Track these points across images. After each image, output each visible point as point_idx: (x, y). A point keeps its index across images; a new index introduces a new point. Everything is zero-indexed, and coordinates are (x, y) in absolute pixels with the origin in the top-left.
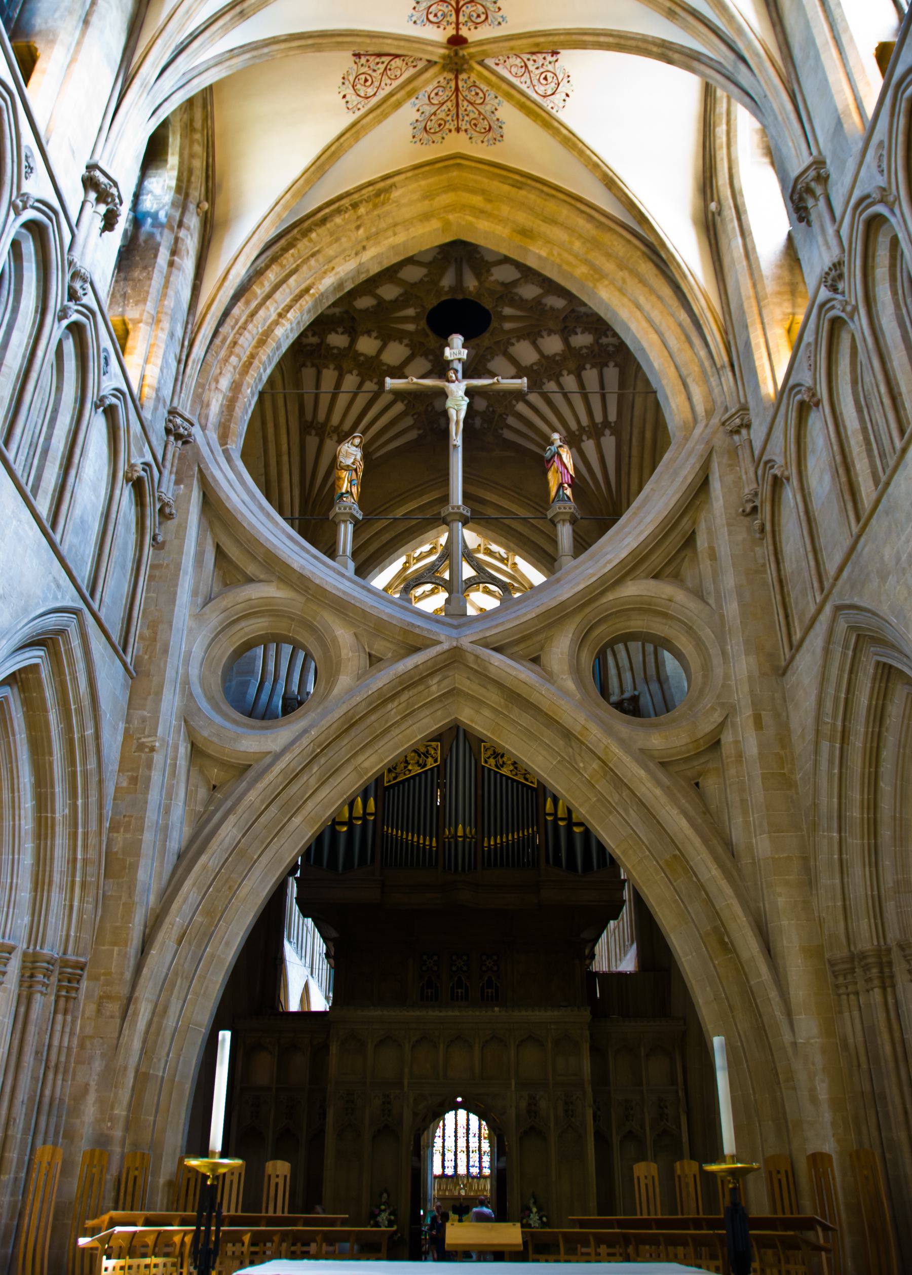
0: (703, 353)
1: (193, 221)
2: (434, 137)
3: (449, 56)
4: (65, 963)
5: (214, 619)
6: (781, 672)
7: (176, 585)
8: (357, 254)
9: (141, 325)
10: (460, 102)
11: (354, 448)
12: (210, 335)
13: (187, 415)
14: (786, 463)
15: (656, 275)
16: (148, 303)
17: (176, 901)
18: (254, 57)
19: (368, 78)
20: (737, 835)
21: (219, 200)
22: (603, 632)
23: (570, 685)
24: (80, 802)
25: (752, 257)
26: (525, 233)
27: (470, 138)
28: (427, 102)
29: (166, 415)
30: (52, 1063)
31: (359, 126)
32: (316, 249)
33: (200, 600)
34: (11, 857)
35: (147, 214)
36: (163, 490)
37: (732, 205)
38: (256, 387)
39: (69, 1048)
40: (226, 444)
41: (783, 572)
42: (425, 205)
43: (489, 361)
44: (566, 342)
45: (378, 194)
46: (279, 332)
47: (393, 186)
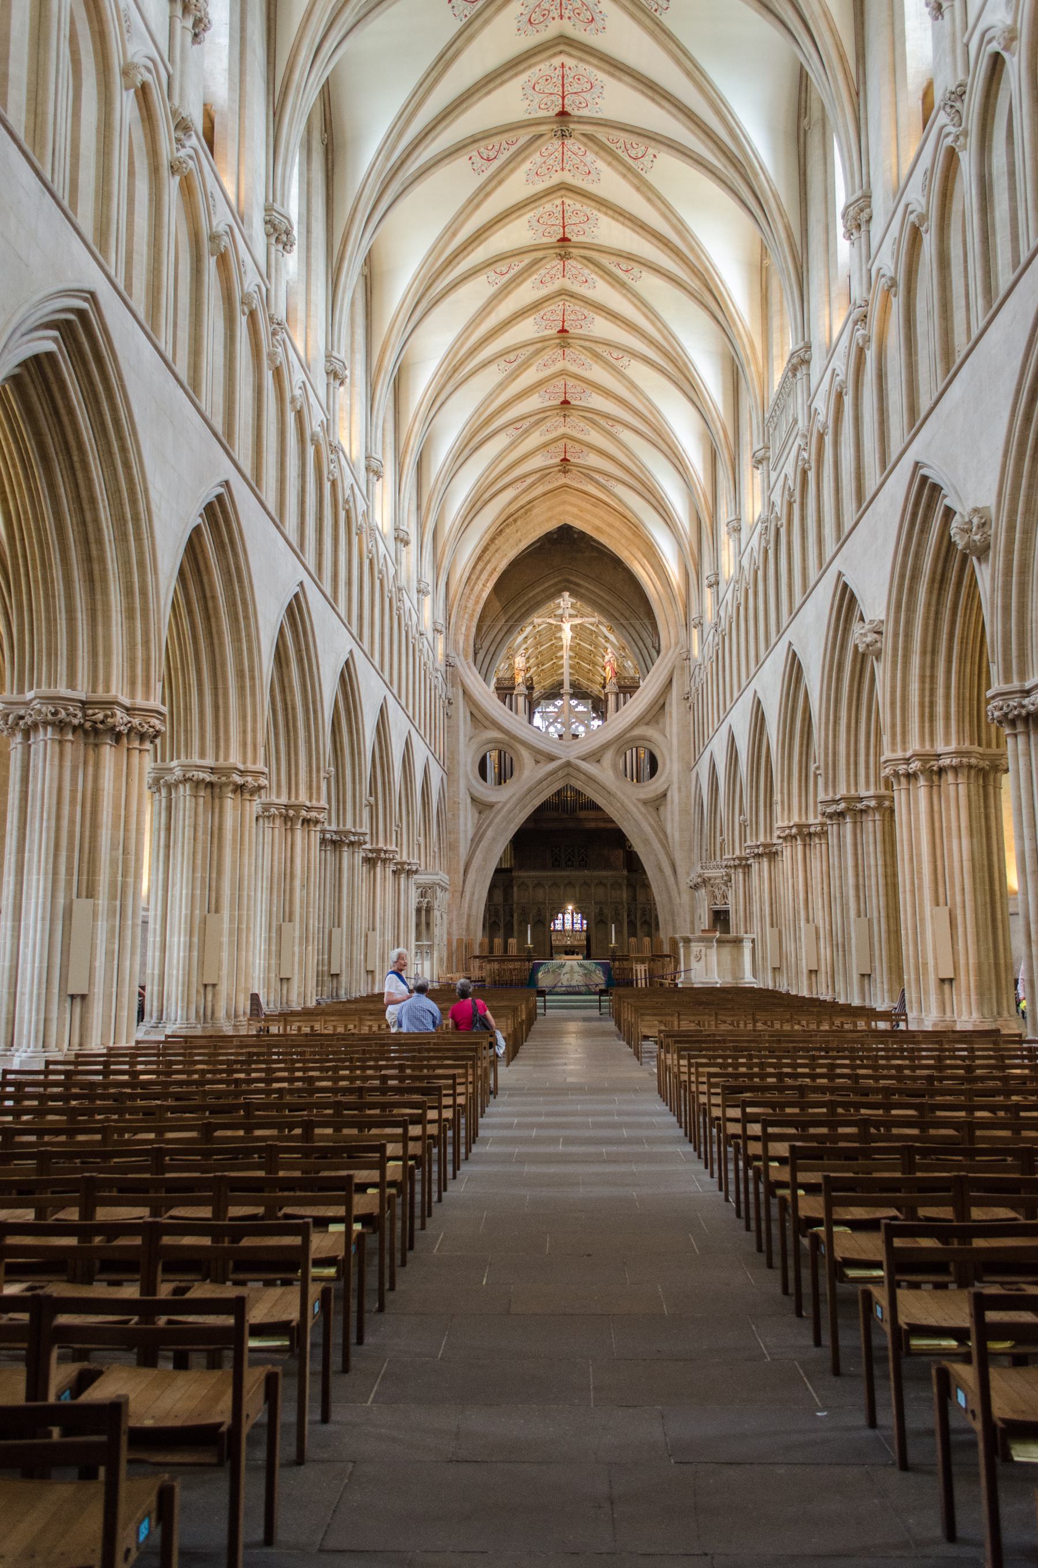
23: (610, 773)
26: (598, 529)
42: (550, 514)
45: (526, 513)
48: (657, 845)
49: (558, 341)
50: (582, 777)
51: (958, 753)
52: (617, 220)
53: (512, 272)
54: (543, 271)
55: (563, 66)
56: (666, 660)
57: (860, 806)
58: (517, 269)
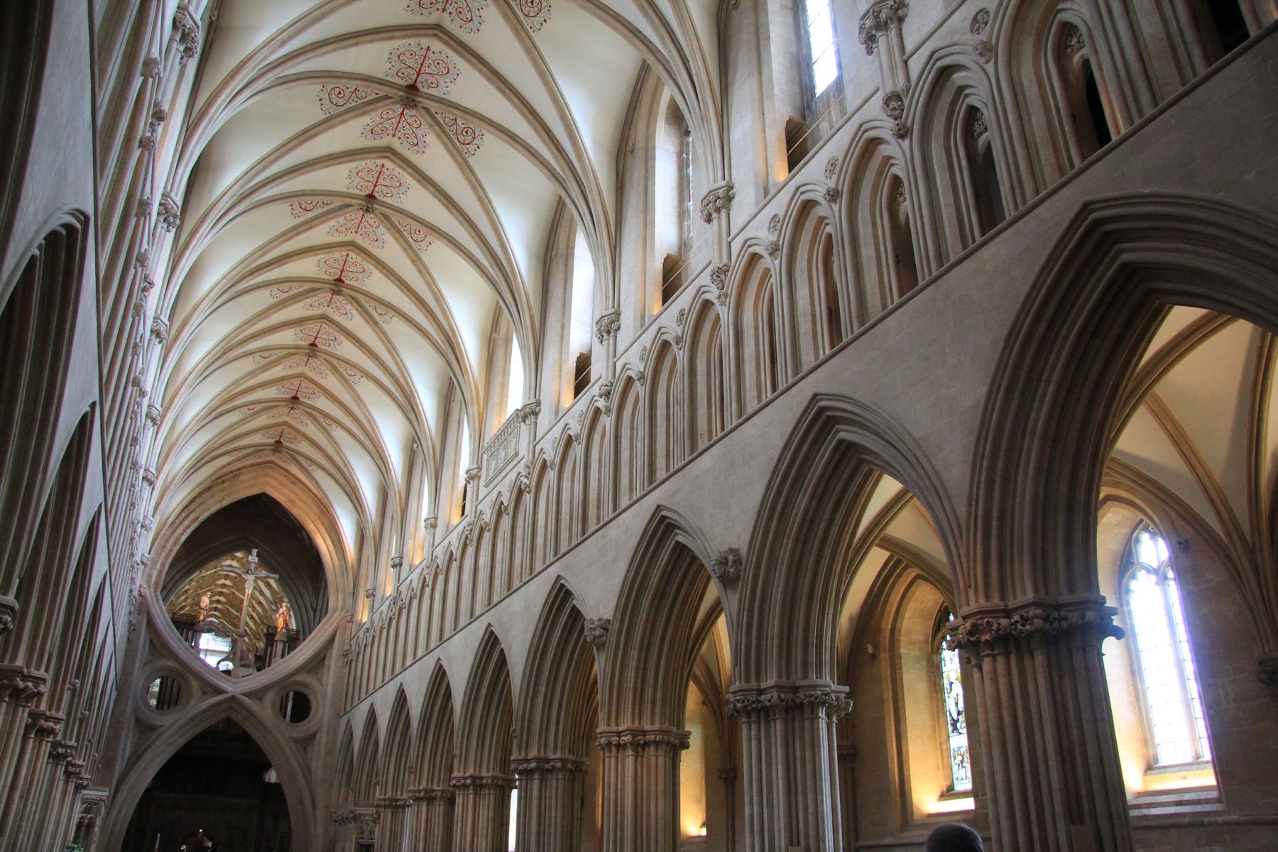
0: (346, 582)
20: (313, 768)
23: (269, 711)
26: (292, 502)
45: (234, 477)
48: (301, 781)
49: (307, 351)
51: (661, 732)
52: (389, 278)
53: (291, 293)
54: (315, 298)
55: (383, 166)
56: (332, 620)
57: (547, 766)
58: (296, 291)
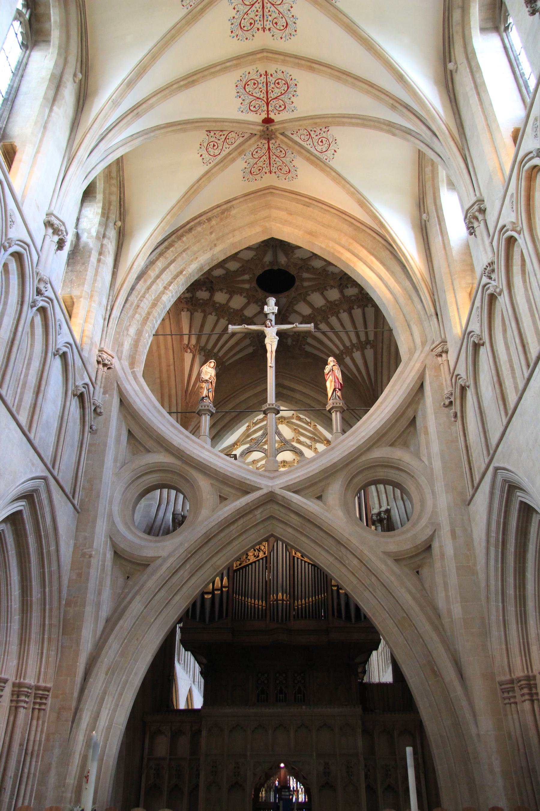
0: (419, 306)
1: (112, 234)
2: (257, 177)
3: (263, 131)
4: (38, 688)
5: (127, 476)
6: (467, 503)
7: (104, 456)
8: (211, 249)
9: (82, 299)
10: (271, 156)
11: (211, 369)
12: (123, 302)
13: (110, 352)
14: (467, 377)
15: (391, 259)
16: (86, 286)
17: (105, 649)
18: (145, 139)
19: (215, 144)
20: (441, 604)
21: (128, 219)
22: (360, 480)
23: (340, 513)
24: (47, 590)
25: (447, 249)
26: (311, 233)
27: (278, 177)
28: (251, 157)
29: (97, 352)
30: (30, 751)
31: (210, 174)
32: (186, 247)
33: (118, 465)
34: (6, 625)
35: (84, 230)
36: (95, 398)
37: (436, 216)
38: (151, 332)
39: (40, 741)
40: (134, 368)
41: (468, 442)
43: (295, 305)
44: (341, 292)
45: (223, 213)
46: (165, 298)
47: (232, 207)
50: (294, 519)
